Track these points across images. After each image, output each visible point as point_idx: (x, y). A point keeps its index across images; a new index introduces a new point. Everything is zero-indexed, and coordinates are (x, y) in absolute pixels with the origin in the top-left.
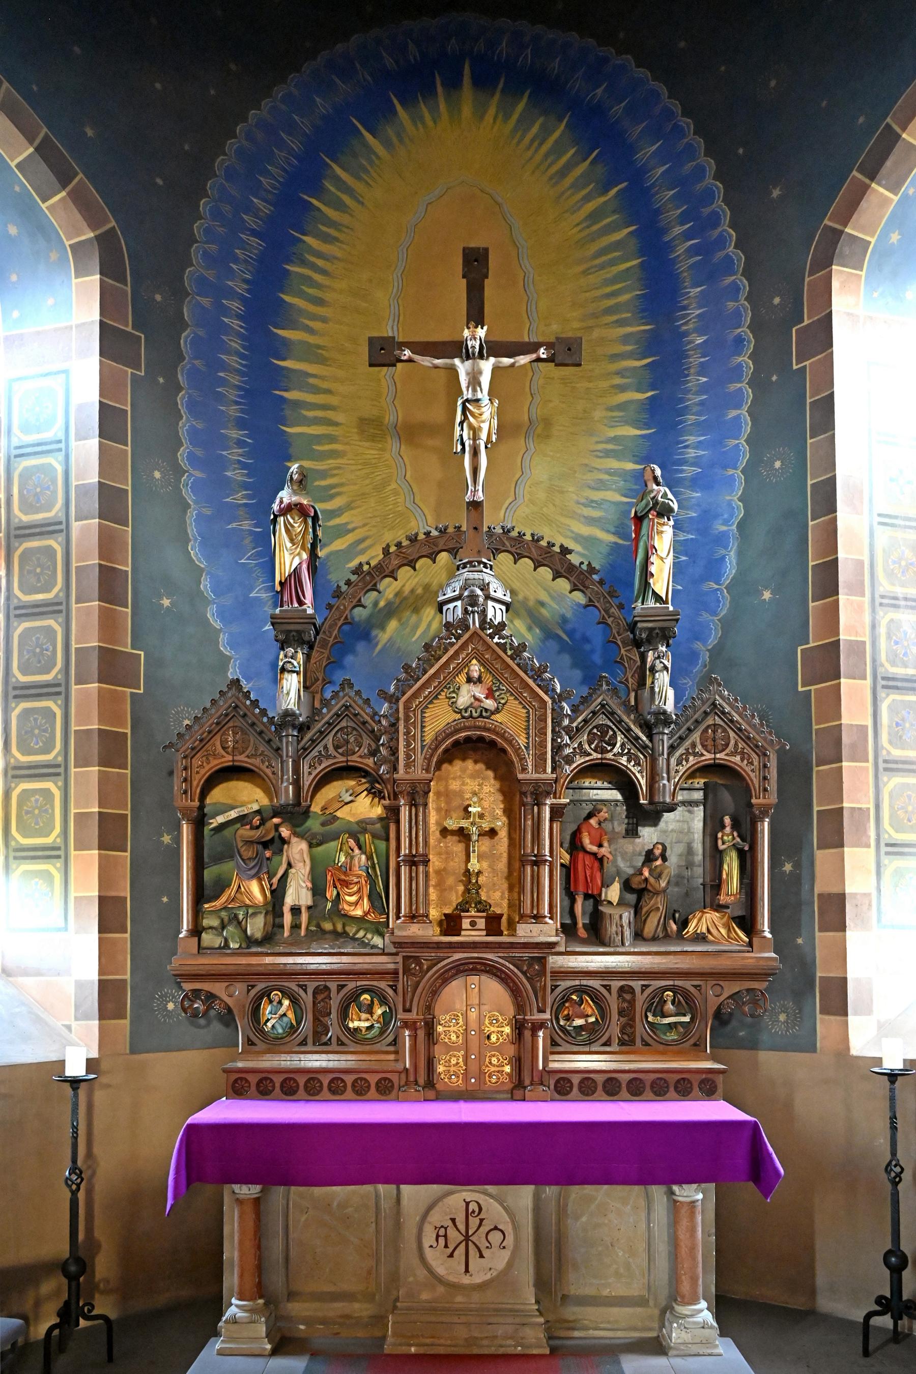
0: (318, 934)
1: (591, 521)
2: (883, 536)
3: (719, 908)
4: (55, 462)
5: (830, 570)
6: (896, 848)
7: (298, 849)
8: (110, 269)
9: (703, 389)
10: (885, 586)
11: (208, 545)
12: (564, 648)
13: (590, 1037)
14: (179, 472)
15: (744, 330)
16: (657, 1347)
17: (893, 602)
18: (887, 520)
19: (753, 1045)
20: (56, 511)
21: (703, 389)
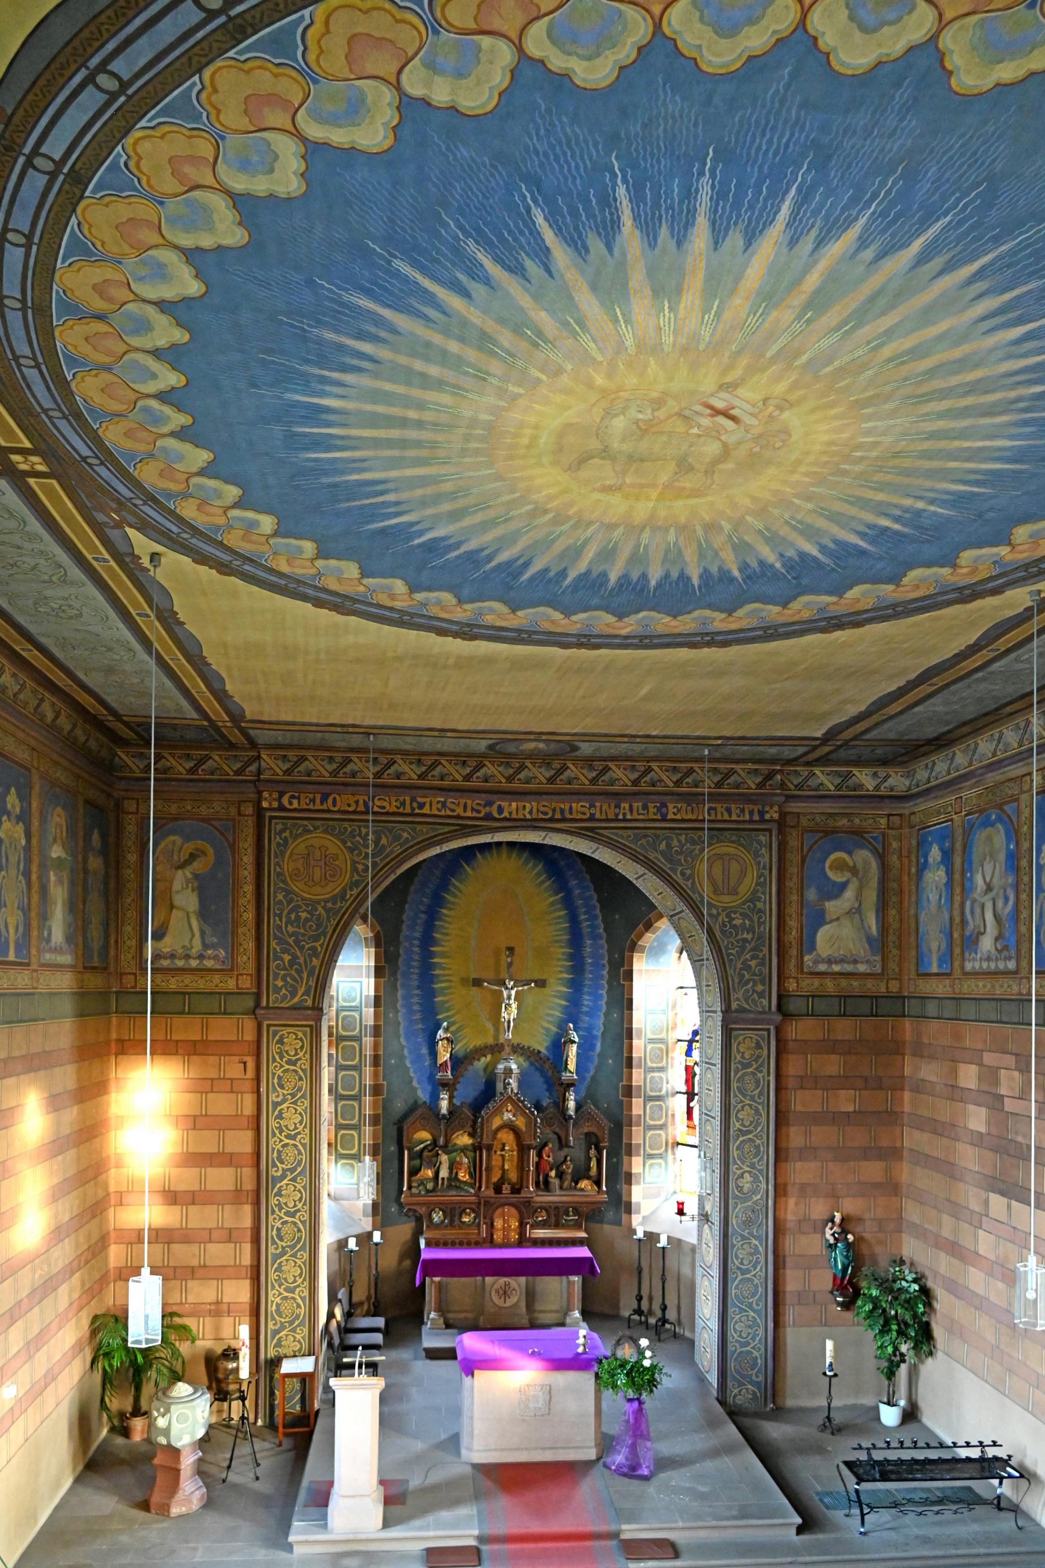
0: (450, 1187)
1: (549, 1022)
2: (649, 1047)
3: (589, 1178)
4: (356, 1015)
5: (630, 1059)
6: (651, 1156)
7: (444, 1158)
8: (378, 945)
9: (590, 979)
10: (650, 1064)
11: (408, 1038)
12: (537, 1069)
13: (544, 1225)
14: (397, 1011)
15: (605, 962)
16: (562, 1324)
17: (653, 1070)
18: (652, 1041)
19: (601, 1222)
20: (356, 1032)
21: (590, 979)
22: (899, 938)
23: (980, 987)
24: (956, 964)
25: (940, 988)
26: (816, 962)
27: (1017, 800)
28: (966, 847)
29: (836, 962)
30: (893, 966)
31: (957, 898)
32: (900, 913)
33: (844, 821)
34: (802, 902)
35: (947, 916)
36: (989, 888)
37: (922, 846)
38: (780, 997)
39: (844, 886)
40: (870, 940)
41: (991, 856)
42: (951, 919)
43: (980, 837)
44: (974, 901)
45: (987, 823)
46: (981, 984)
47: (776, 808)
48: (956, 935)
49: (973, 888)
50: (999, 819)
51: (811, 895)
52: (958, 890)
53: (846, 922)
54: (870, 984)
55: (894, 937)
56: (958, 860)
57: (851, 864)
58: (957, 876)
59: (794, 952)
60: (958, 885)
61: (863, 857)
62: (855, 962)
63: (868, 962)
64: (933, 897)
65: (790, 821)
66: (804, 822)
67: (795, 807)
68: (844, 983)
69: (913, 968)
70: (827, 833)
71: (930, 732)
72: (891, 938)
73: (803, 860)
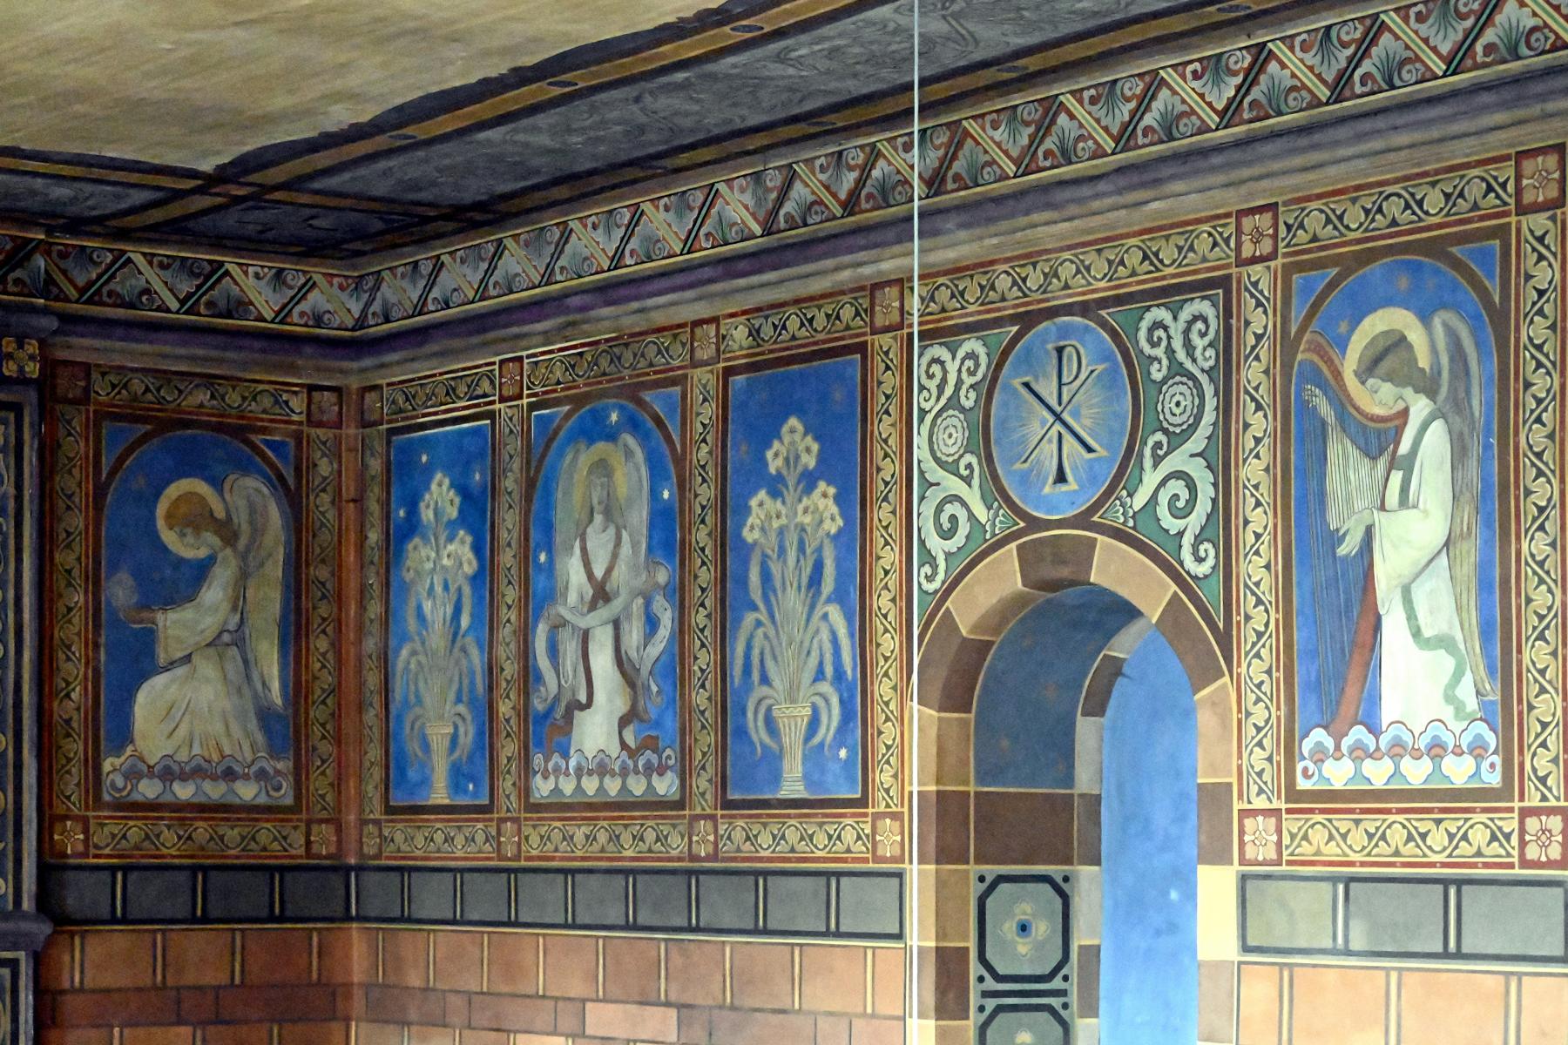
22: (336, 716)
23: (579, 842)
24: (507, 785)
25: (466, 844)
26: (133, 775)
27: (681, 381)
28: (537, 486)
29: (184, 777)
30: (319, 784)
31: (510, 616)
32: (336, 646)
33: (202, 396)
34: (96, 612)
35: (477, 658)
36: (601, 594)
37: (404, 478)
38: (46, 871)
39: (201, 571)
40: (265, 716)
41: (608, 514)
42: (491, 669)
43: (577, 463)
44: (558, 625)
45: (596, 431)
46: (580, 834)
47: (32, 347)
48: (504, 709)
49: (552, 595)
50: (634, 425)
51: (121, 591)
52: (511, 595)
53: (206, 667)
54: (266, 832)
55: (325, 706)
56: (509, 521)
57: (220, 514)
58: (507, 558)
59: (75, 747)
60: (511, 583)
61: (249, 497)
62: (230, 775)
63: (262, 775)
64: (437, 611)
65: (67, 385)
66: (102, 391)
67: (82, 348)
68: (202, 831)
69: (372, 790)
70: (166, 425)
71: (473, 190)
72: (318, 713)
73: (100, 492)
